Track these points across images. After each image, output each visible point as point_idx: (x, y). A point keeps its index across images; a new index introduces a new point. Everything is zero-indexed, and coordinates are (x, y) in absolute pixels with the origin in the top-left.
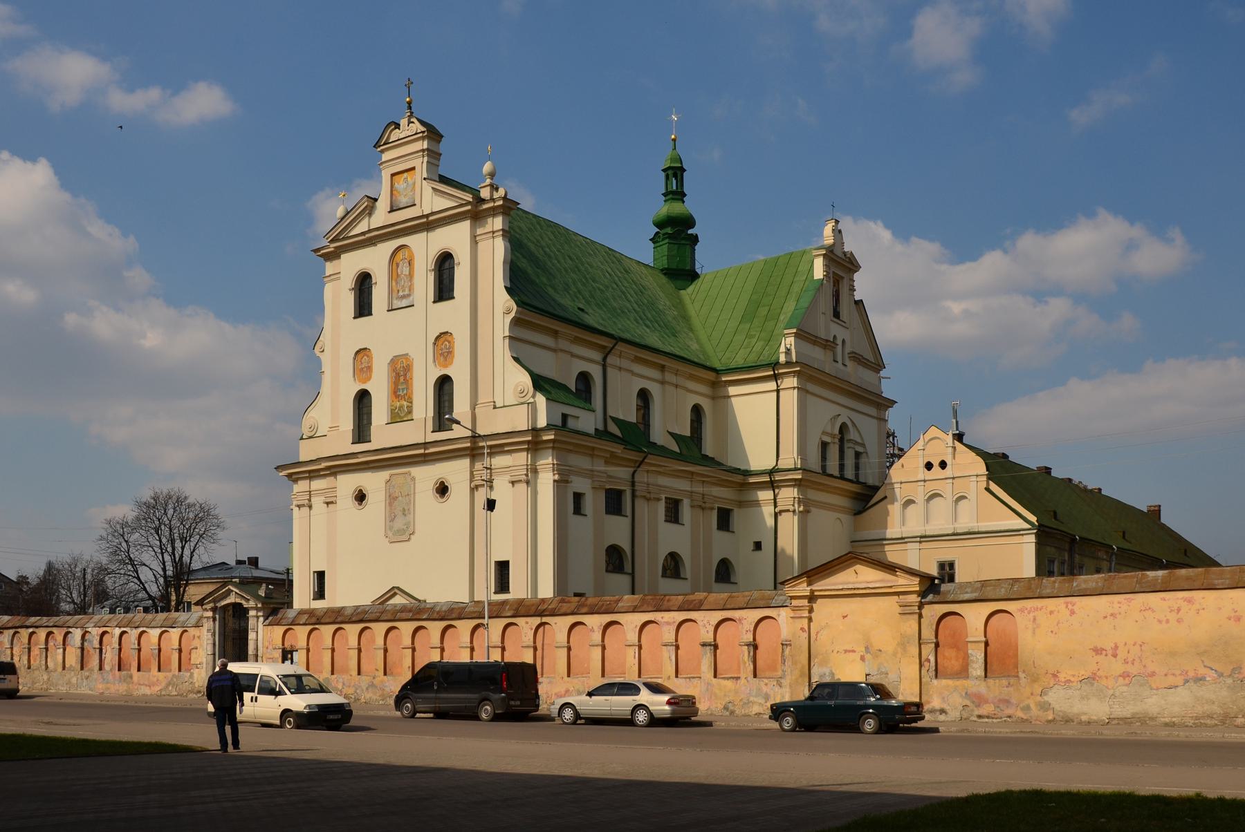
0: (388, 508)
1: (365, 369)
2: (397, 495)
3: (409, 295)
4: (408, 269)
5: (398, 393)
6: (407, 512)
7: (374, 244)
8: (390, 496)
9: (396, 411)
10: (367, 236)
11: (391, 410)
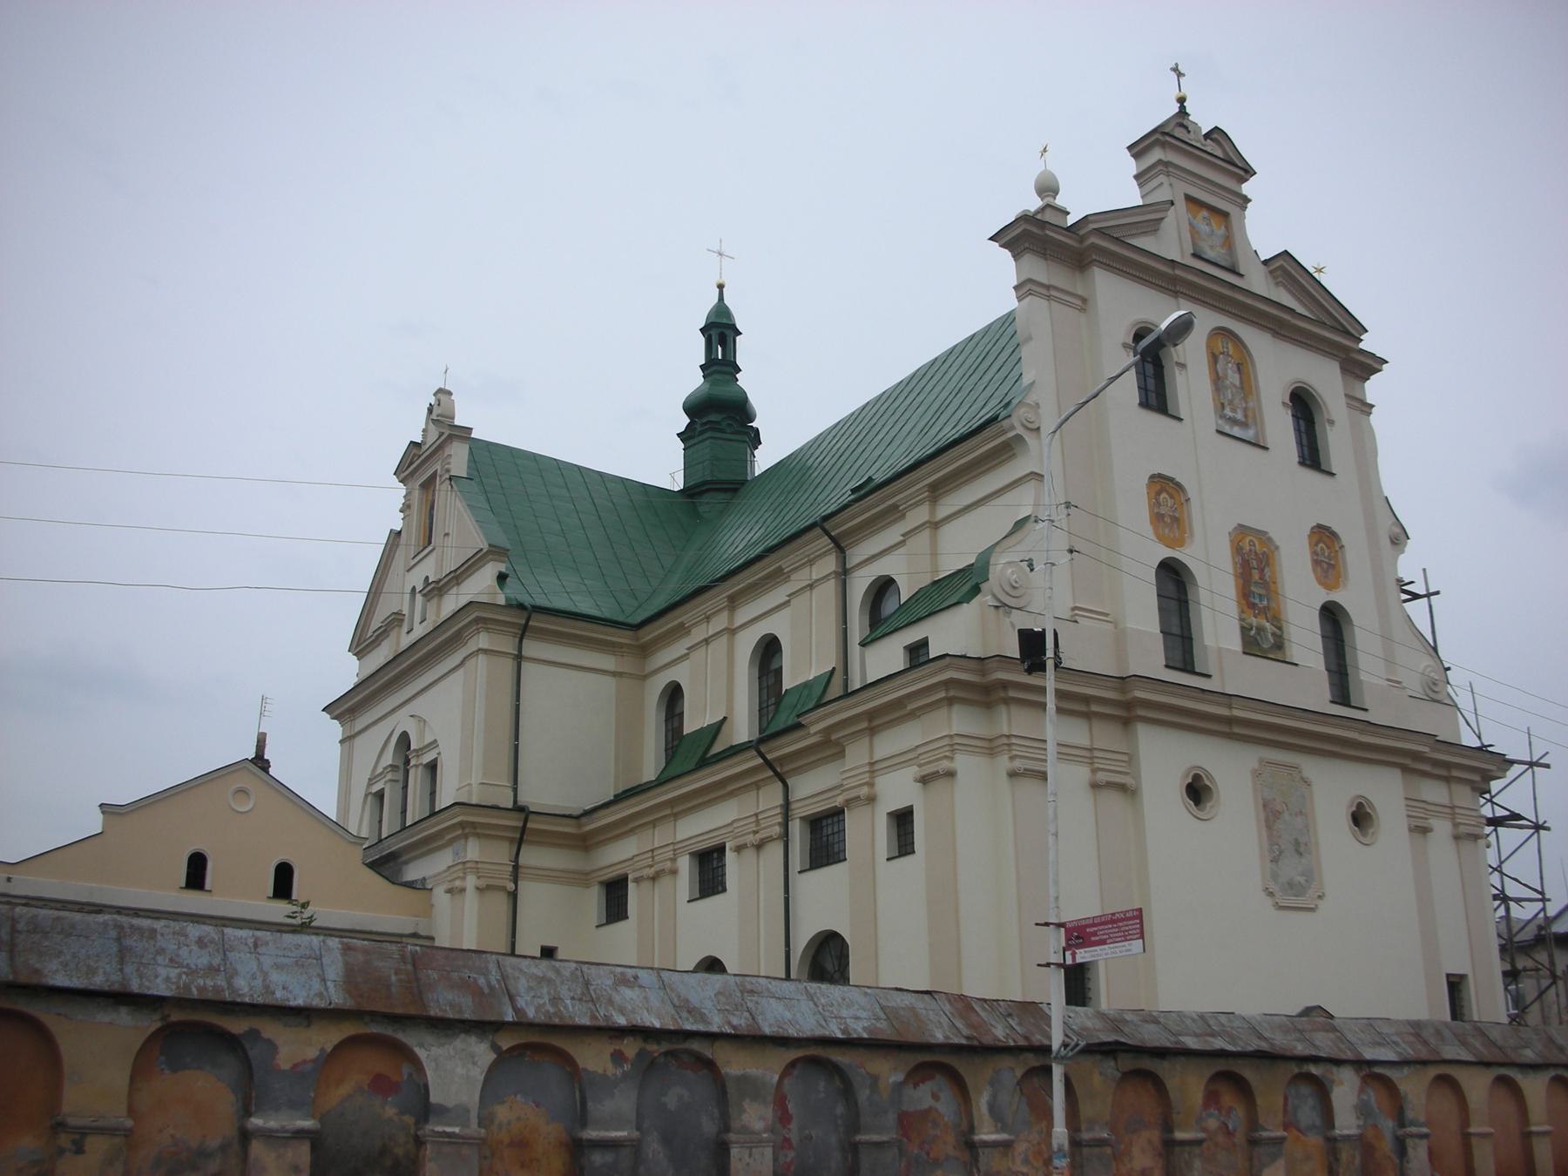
0: (1264, 833)
1: (1168, 520)
2: (1278, 808)
3: (1244, 425)
4: (1237, 376)
5: (1252, 600)
6: (1302, 850)
8: (1265, 806)
9: (1253, 633)
10: (1178, 272)
11: (1243, 628)
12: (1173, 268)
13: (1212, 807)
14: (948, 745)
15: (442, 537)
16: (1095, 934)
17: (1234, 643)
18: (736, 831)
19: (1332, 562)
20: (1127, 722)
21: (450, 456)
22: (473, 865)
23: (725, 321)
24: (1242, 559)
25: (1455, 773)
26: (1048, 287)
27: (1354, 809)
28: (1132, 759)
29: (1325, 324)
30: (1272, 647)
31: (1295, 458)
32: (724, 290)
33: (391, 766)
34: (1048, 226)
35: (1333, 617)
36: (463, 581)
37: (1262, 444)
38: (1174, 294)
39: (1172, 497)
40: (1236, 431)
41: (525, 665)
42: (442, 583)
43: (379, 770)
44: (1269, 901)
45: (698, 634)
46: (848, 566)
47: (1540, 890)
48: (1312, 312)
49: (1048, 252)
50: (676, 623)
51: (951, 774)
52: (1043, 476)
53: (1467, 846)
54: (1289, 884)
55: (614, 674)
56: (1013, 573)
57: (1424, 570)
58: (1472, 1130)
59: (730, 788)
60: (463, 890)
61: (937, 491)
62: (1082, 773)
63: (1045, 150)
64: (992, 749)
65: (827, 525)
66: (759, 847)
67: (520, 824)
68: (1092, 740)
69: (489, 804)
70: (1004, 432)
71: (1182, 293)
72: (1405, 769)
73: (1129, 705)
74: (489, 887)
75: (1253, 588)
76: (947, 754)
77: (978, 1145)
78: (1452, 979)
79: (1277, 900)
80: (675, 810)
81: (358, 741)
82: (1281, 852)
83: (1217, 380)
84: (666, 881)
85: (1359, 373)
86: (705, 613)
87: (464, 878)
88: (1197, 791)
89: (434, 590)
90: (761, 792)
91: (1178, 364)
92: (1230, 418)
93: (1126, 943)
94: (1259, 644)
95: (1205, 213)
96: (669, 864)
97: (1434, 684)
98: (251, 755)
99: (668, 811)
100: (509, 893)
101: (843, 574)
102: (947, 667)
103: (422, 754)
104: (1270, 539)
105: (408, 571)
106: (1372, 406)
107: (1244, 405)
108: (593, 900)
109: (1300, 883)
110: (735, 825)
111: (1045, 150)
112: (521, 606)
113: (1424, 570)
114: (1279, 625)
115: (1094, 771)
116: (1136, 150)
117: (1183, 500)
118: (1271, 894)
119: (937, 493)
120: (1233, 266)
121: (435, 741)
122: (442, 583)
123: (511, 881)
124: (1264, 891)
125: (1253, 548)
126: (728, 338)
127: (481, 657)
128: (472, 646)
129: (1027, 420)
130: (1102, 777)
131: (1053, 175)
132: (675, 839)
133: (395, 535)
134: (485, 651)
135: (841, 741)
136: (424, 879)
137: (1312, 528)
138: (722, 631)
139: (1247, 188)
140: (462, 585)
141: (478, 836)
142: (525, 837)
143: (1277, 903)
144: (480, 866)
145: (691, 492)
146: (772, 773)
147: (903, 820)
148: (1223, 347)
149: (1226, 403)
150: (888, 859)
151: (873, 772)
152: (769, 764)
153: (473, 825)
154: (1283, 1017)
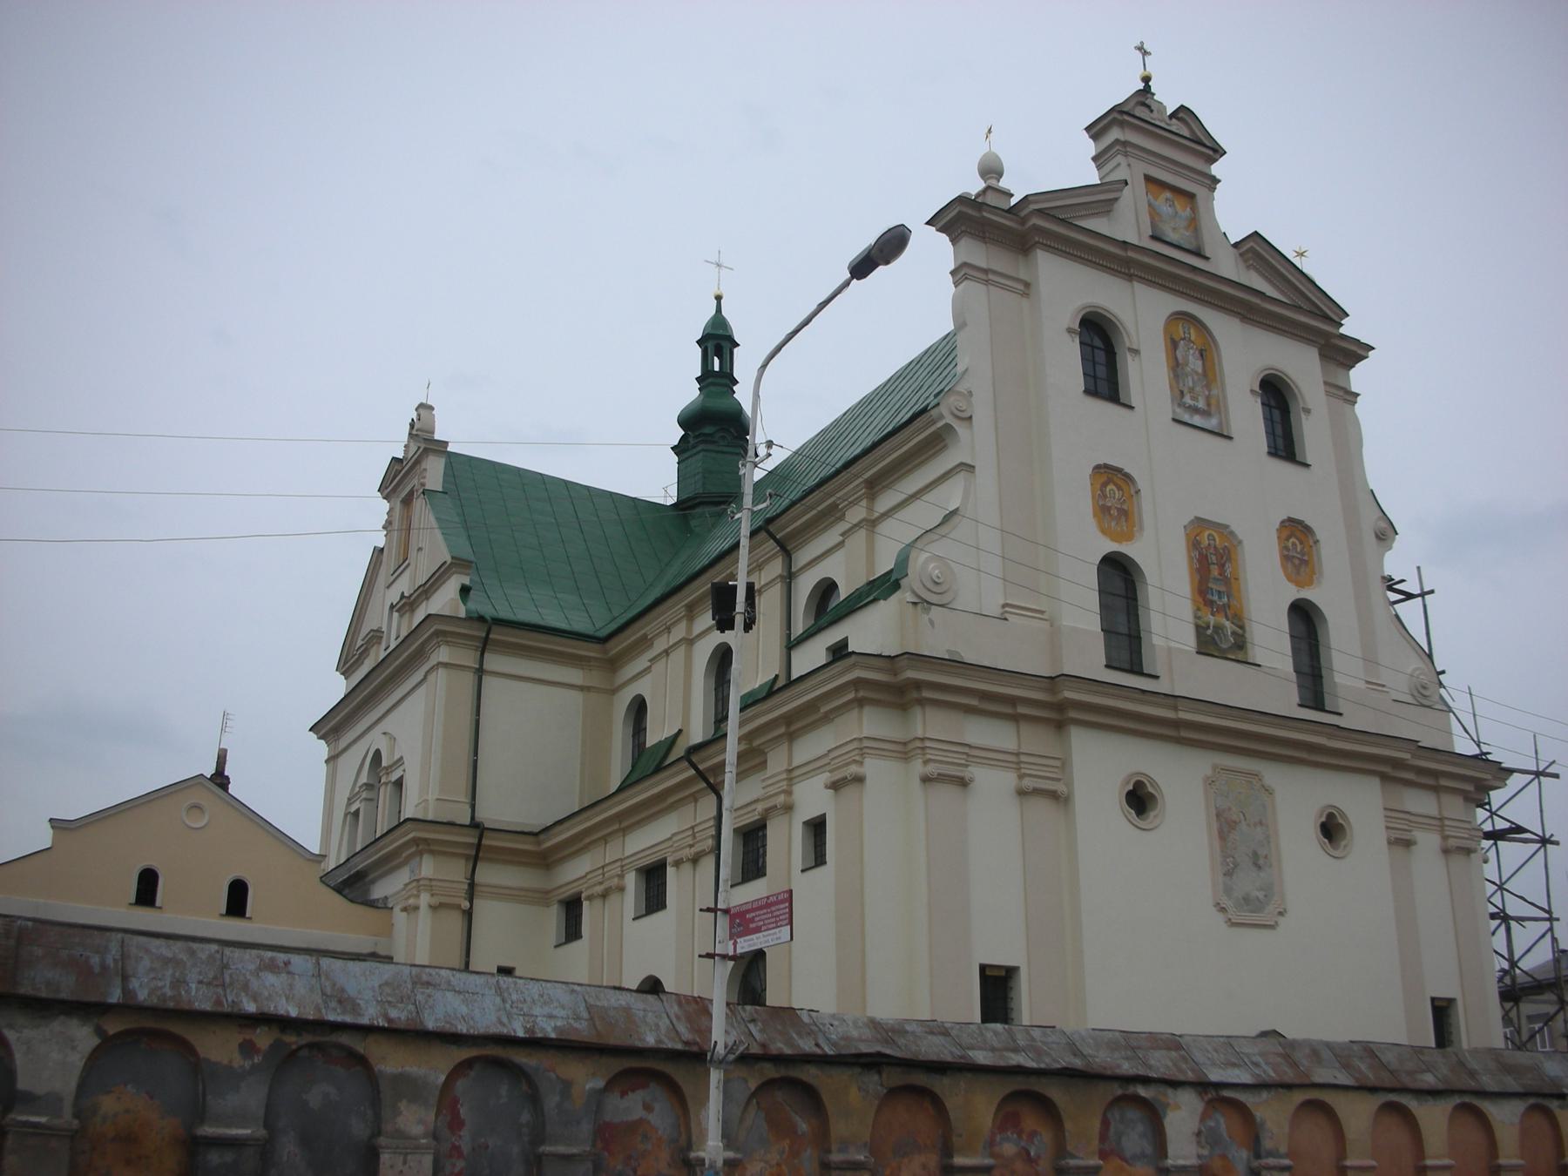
0: (1217, 843)
1: (1114, 512)
2: (1234, 817)
3: (1206, 413)
4: (1200, 363)
5: (1209, 597)
6: (1261, 862)
7: (1130, 277)
8: (1218, 815)
9: (1209, 632)
10: (1131, 254)
11: (1198, 627)
12: (1126, 250)
13: (1155, 816)
14: (857, 748)
15: (416, 551)
16: (752, 920)
17: (1189, 640)
18: (676, 845)
19: (1306, 558)
20: (1060, 726)
21: (425, 470)
22: (427, 882)
23: (721, 332)
24: (1199, 554)
25: (1444, 782)
26: (986, 271)
27: (1323, 819)
28: (1064, 764)
29: (1301, 308)
30: (1231, 647)
31: (1263, 446)
32: (722, 301)
33: (365, 784)
34: (985, 207)
35: (1305, 618)
36: (430, 597)
37: (1225, 434)
38: (1127, 277)
39: (1119, 488)
40: (1197, 420)
41: (486, 680)
42: (412, 598)
43: (357, 789)
44: (1220, 917)
45: (660, 645)
46: (793, 570)
47: (1547, 908)
48: (1288, 297)
49: (987, 235)
50: (638, 635)
51: (859, 780)
52: (973, 467)
53: (1458, 861)
54: (1244, 899)
55: (581, 688)
56: (934, 568)
57: (1419, 568)
58: (1348, 1163)
59: (671, 800)
60: (416, 908)
61: (874, 486)
62: (1008, 780)
63: (990, 131)
64: (905, 753)
65: (771, 528)
66: (695, 860)
67: (475, 841)
68: (1019, 746)
69: (445, 821)
70: (934, 422)
71: (1137, 276)
72: (1384, 778)
73: (1061, 707)
74: (442, 906)
75: (1210, 585)
76: (857, 758)
77: (694, 1162)
78: (1436, 1003)
79: (1230, 917)
80: (623, 825)
81: (341, 760)
82: (1236, 865)
83: (1176, 367)
84: (614, 899)
85: (1341, 360)
86: (666, 624)
87: (418, 896)
88: (1139, 800)
89: (406, 605)
90: (699, 804)
91: (1131, 350)
92: (1190, 407)
93: (777, 930)
94: (1216, 644)
95: (1168, 194)
96: (616, 880)
97: (1424, 688)
98: (209, 770)
99: (616, 827)
100: (464, 912)
101: (789, 578)
102: (854, 666)
103: (391, 772)
104: (1232, 533)
105: (388, 587)
106: (1358, 395)
107: (1207, 393)
108: (553, 918)
109: (1257, 898)
110: (675, 839)
111: (990, 131)
112: (481, 619)
113: (1419, 568)
114: (1240, 623)
115: (1021, 777)
116: (1095, 130)
117: (1132, 492)
118: (1223, 910)
119: (877, 489)
120: (1199, 248)
121: (401, 758)
122: (412, 598)
123: (466, 899)
124: (1215, 906)
125: (1212, 542)
126: (724, 351)
127: (441, 671)
128: (433, 661)
129: (957, 409)
130: (1028, 783)
131: (997, 156)
132: (623, 854)
133: (378, 552)
134: (446, 665)
135: (762, 747)
136: (386, 898)
137: (1283, 522)
138: (681, 640)
139: (1216, 169)
140: (431, 599)
141: (432, 852)
142: (481, 855)
143: (1230, 919)
144: (434, 883)
145: (684, 506)
146: (705, 785)
147: (817, 827)
148: (1184, 333)
149: (1186, 391)
150: (803, 871)
151: (791, 779)
152: (701, 775)
153: (426, 840)
154: (1117, 1034)
